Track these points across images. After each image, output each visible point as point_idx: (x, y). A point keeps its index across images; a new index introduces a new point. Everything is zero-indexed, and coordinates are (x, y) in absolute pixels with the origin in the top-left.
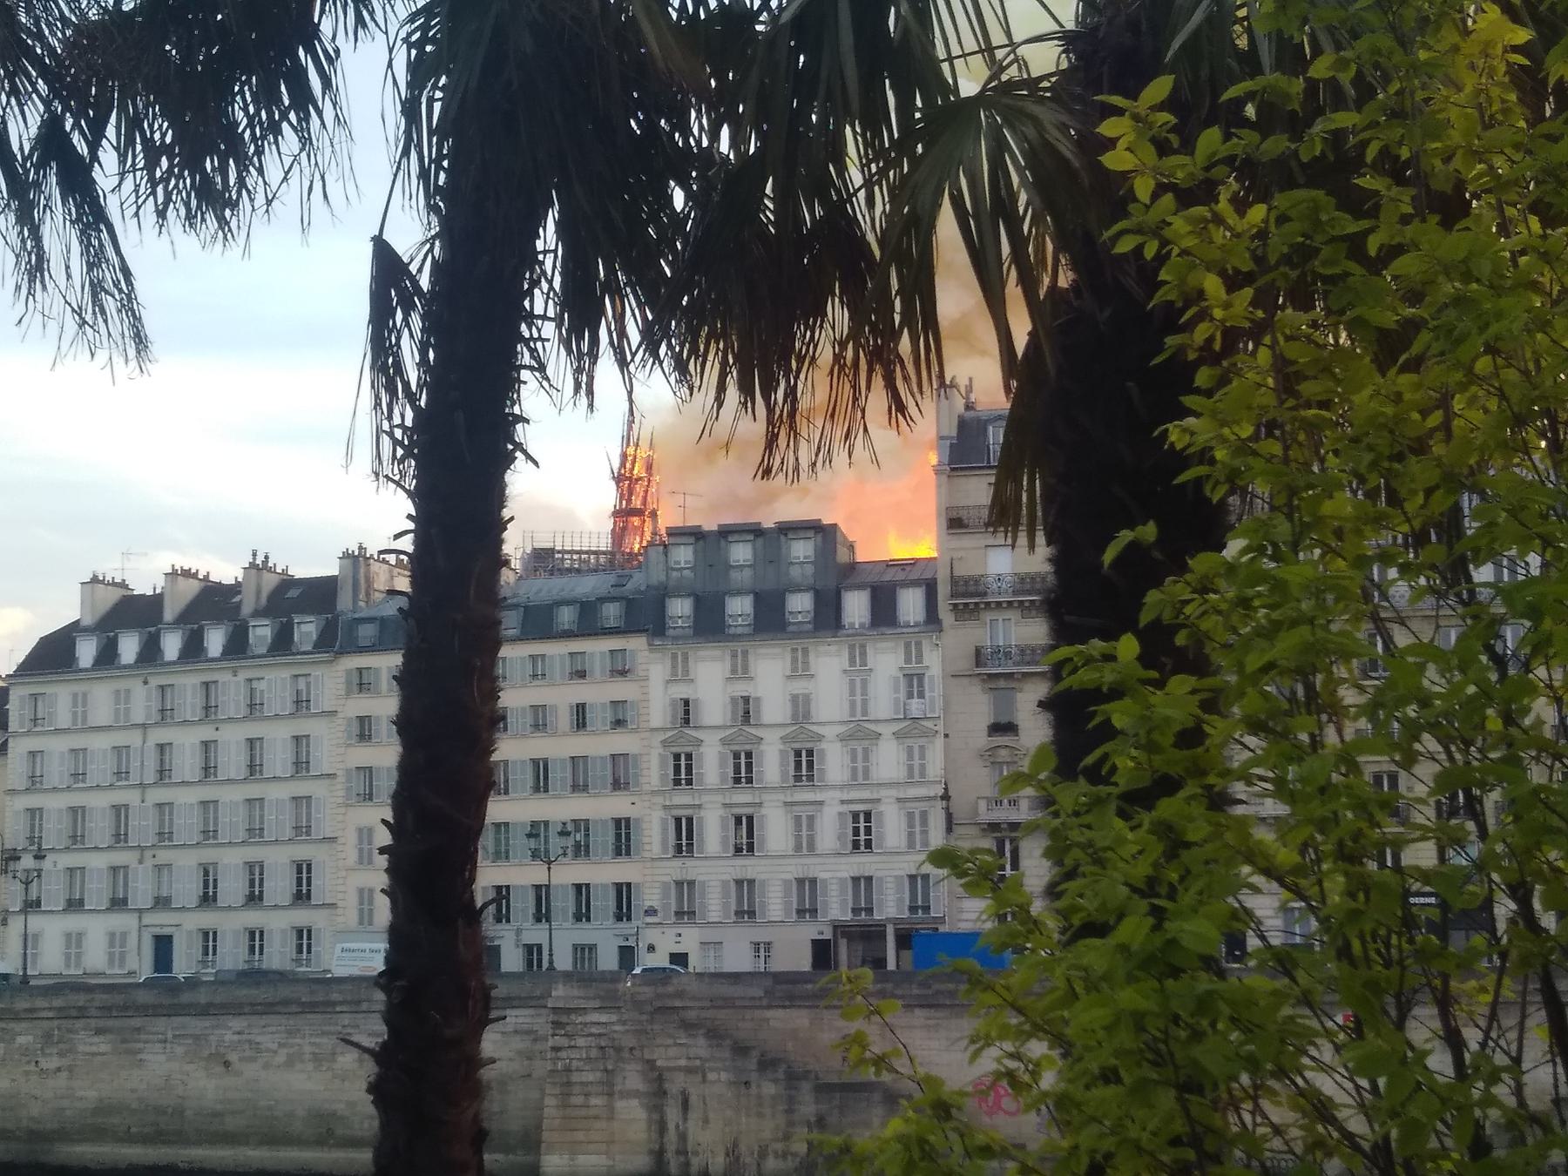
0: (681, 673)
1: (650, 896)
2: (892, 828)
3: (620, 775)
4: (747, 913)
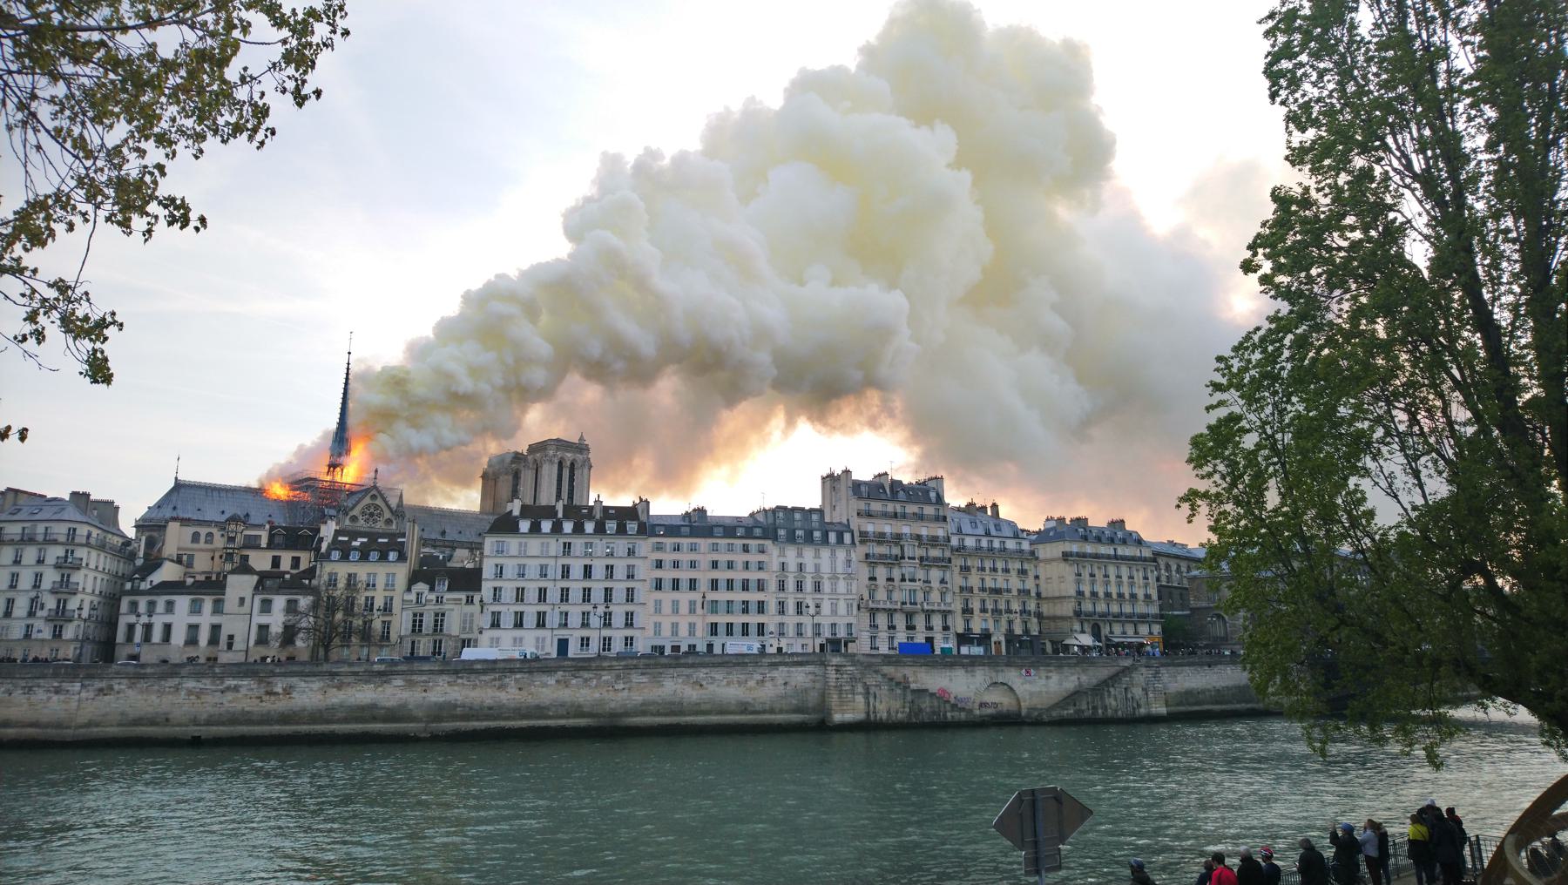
0: (782, 554)
3: (761, 586)
4: (800, 634)
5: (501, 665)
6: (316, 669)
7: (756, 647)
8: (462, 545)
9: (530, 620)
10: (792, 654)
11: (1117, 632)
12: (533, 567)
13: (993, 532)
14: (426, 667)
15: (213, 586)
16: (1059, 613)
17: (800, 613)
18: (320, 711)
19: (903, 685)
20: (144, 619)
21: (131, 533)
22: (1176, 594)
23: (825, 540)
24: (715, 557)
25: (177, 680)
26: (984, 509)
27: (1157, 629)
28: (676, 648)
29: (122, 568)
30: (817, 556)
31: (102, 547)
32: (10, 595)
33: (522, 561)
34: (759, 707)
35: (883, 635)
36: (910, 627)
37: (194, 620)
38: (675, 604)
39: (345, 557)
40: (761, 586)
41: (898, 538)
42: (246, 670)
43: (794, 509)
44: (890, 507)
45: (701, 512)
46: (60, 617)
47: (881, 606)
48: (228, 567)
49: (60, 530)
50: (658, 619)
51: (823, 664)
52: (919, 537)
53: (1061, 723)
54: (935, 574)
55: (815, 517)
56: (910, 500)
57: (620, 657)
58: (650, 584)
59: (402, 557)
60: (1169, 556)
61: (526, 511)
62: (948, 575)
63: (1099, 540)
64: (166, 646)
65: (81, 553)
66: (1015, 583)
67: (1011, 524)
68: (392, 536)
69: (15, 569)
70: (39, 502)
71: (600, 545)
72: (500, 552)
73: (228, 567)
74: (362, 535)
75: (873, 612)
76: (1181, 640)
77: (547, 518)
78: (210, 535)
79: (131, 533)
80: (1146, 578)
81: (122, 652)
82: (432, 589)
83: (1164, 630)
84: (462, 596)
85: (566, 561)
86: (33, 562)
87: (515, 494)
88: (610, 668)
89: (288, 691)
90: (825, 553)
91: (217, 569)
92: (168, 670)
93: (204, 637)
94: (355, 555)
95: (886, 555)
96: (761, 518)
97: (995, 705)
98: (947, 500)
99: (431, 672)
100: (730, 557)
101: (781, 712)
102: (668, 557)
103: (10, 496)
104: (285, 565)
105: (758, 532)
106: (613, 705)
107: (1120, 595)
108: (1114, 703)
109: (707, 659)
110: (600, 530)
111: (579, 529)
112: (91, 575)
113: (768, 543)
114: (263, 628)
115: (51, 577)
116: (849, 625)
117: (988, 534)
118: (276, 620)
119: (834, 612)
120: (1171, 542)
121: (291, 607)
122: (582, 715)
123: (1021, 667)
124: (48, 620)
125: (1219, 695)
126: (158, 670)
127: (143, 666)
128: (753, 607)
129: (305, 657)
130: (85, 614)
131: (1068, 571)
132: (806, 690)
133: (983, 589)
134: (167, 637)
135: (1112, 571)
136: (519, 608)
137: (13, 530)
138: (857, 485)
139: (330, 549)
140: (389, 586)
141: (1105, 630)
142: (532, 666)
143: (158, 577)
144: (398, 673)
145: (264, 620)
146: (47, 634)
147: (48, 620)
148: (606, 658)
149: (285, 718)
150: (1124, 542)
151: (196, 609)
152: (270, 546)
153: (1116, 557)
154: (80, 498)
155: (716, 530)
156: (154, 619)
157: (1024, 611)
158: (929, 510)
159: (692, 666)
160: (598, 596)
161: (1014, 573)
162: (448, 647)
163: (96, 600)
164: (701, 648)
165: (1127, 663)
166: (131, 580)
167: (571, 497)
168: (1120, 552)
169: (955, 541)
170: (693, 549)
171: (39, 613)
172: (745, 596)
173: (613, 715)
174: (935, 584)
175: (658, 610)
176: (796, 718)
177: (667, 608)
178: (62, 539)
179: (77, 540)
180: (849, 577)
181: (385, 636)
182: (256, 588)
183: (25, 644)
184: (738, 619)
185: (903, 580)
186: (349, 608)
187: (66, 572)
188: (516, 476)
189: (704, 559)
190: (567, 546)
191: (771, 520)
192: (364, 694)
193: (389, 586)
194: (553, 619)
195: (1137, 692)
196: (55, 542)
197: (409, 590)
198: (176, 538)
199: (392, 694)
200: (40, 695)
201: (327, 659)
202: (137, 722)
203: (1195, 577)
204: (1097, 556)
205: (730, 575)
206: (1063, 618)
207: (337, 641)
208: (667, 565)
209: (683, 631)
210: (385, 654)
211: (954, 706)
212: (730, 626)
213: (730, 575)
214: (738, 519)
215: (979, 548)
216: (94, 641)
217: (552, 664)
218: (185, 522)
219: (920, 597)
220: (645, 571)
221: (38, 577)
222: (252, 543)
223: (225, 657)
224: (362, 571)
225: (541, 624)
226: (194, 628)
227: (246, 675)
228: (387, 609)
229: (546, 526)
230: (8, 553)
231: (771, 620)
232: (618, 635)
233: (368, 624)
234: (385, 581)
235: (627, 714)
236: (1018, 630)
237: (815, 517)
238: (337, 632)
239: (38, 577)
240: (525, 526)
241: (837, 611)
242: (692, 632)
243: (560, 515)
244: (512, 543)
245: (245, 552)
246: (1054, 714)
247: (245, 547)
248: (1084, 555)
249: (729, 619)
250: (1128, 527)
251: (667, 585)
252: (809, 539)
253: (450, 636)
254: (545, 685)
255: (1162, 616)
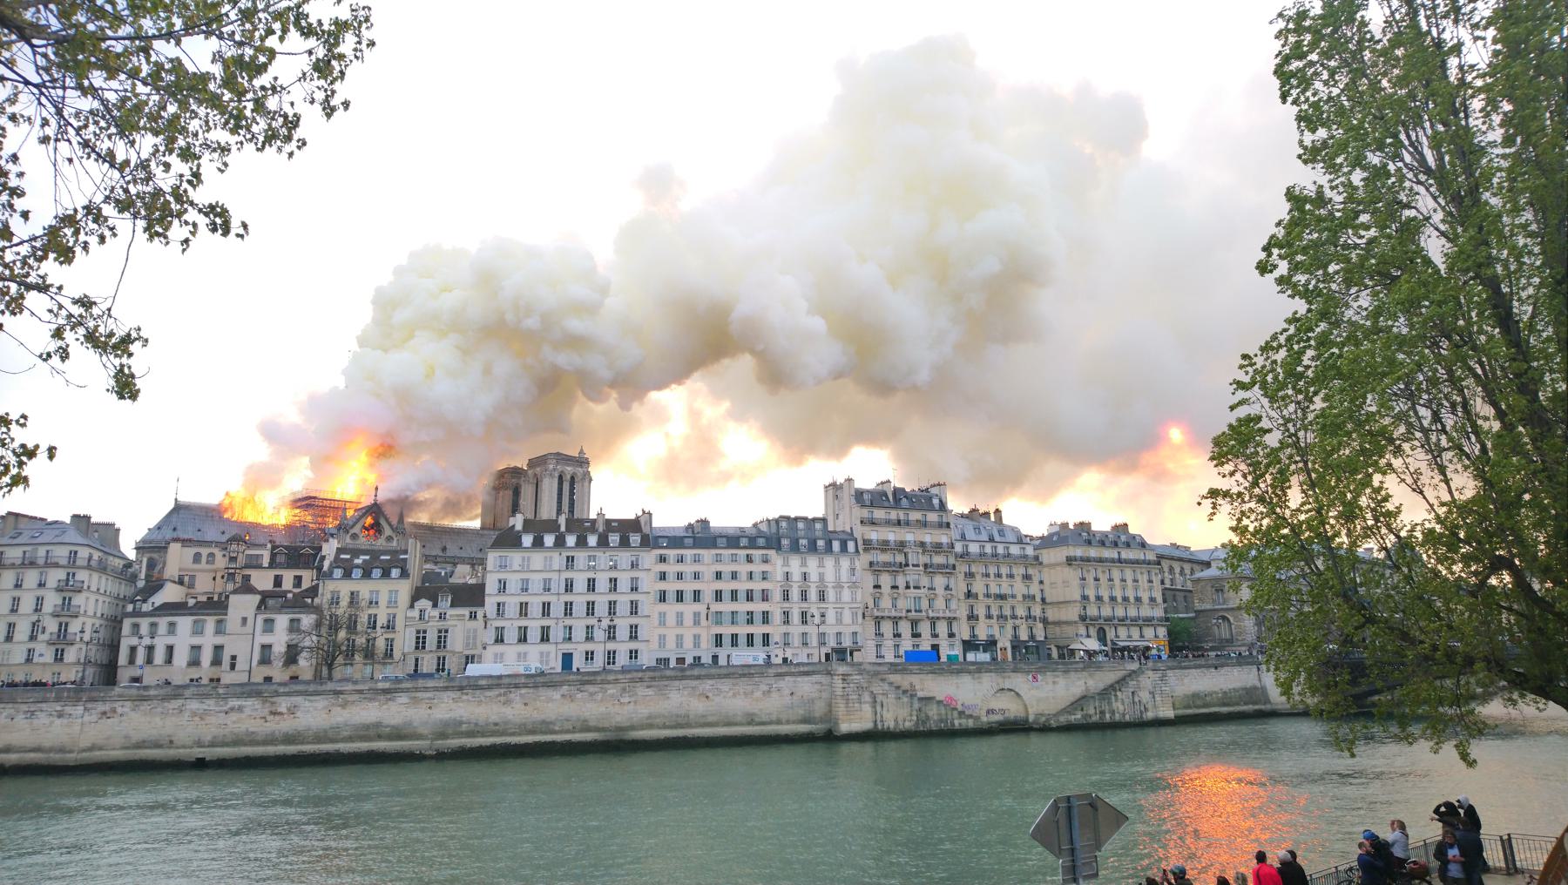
0: (786, 564)
1: (776, 638)
2: (847, 617)
3: (765, 597)
4: (805, 644)
5: (506, 681)
6: (320, 688)
7: (761, 657)
8: (463, 561)
9: (534, 635)
10: (798, 664)
11: (1125, 636)
12: (536, 581)
13: (997, 538)
14: (430, 683)
15: (216, 606)
16: (1064, 618)
17: (804, 622)
18: (325, 731)
19: (910, 693)
20: (147, 641)
21: (131, 554)
22: (1180, 596)
23: (829, 549)
24: (719, 568)
25: (180, 702)
26: (987, 514)
27: (1162, 632)
28: (681, 661)
29: (125, 590)
30: (821, 565)
31: (102, 568)
32: (12, 619)
33: (525, 576)
34: (765, 719)
35: (889, 643)
36: (916, 635)
37: (196, 641)
38: (680, 616)
39: (347, 575)
40: (765, 597)
41: (901, 546)
42: (248, 690)
43: (796, 519)
44: (893, 515)
45: (704, 523)
46: (62, 639)
47: (886, 614)
48: (230, 587)
49: (61, 553)
50: (662, 631)
51: (829, 673)
52: (922, 544)
53: (1069, 728)
54: (940, 581)
55: (818, 526)
56: (913, 507)
57: (624, 670)
58: (654, 597)
59: (404, 574)
60: (1172, 559)
61: (528, 525)
62: (952, 581)
63: (1102, 544)
64: (168, 668)
65: (82, 575)
66: (1020, 588)
67: (1014, 530)
68: (394, 553)
69: (17, 593)
70: (40, 525)
71: (603, 558)
72: (503, 567)
73: (230, 587)
74: (365, 552)
75: (878, 620)
76: (1187, 643)
77: (550, 532)
78: (212, 555)
79: (131, 554)
80: (1150, 581)
81: (124, 675)
82: (435, 605)
83: (1170, 633)
84: (465, 611)
85: (569, 575)
86: (34, 585)
87: (515, 509)
88: (616, 681)
89: (292, 711)
90: (829, 562)
91: (219, 590)
92: (172, 692)
93: (206, 657)
94: (357, 573)
95: (890, 562)
96: (764, 528)
97: (1003, 711)
98: (950, 506)
99: (436, 689)
100: (734, 567)
101: (788, 722)
102: (671, 568)
103: (12, 519)
104: (287, 584)
105: (761, 542)
106: (618, 719)
107: (1125, 599)
108: (1121, 707)
109: (713, 671)
110: (603, 542)
111: (582, 543)
112: (93, 598)
113: (772, 553)
114: (266, 648)
115: (52, 600)
116: (855, 634)
117: (991, 540)
118: (279, 639)
119: (839, 621)
120: (1174, 545)
121: (294, 626)
122: (588, 729)
123: (1028, 672)
124: (50, 643)
125: (1226, 699)
126: (162, 692)
127: (146, 688)
128: (758, 618)
129: (307, 675)
130: (87, 637)
131: (1072, 575)
132: (812, 701)
133: (988, 596)
134: (169, 660)
135: (1116, 574)
136: (523, 623)
137: (13, 554)
138: (859, 494)
139: (332, 567)
140: (392, 603)
141: (1110, 634)
142: (539, 681)
143: (159, 599)
144: (403, 691)
145: (267, 639)
146: (49, 657)
147: (50, 643)
148: (611, 671)
149: (289, 739)
150: (1128, 545)
151: (198, 630)
152: (273, 565)
153: (1120, 561)
154: (81, 521)
155: (719, 541)
156: (156, 641)
157: (1029, 617)
158: (932, 517)
159: (698, 678)
160: (601, 609)
161: (1018, 579)
162: (452, 664)
163: (98, 622)
164: (706, 659)
165: (1134, 666)
166: (133, 602)
167: (571, 511)
168: (1124, 555)
169: (958, 548)
170: (697, 560)
171: (41, 637)
172: (750, 607)
173: (620, 729)
174: (940, 591)
175: (662, 623)
176: (803, 728)
177: (671, 620)
178: (64, 562)
179: (79, 563)
180: (854, 585)
181: (389, 654)
182: (259, 608)
183: (27, 668)
184: (743, 630)
185: (908, 587)
186: (352, 626)
187: (67, 595)
188: (517, 492)
189: (708, 570)
190: (570, 560)
191: (774, 530)
192: (368, 713)
193: (392, 603)
194: (557, 633)
195: (1144, 696)
196: (56, 565)
197: (412, 606)
198: (177, 559)
199: (396, 712)
200: (42, 719)
201: (330, 678)
202: (140, 745)
203: (1199, 580)
204: (1101, 560)
205: (734, 585)
206: (1067, 623)
207: (340, 660)
208: (671, 576)
209: (688, 643)
210: (389, 671)
211: (961, 713)
212: (734, 638)
213: (734, 585)
214: (742, 529)
215: (983, 555)
216: (96, 664)
217: (557, 679)
218: (186, 542)
219: (924, 604)
220: (649, 583)
221: (39, 601)
222: (254, 564)
223: (228, 678)
224: (365, 589)
225: (545, 638)
226: (196, 649)
227: (250, 695)
228: (390, 626)
229: (549, 540)
230: (9, 577)
231: (776, 630)
232: (622, 648)
233: (371, 642)
234: (388, 597)
235: (633, 728)
236: (1024, 636)
237: (818, 526)
238: (340, 650)
239: (39, 601)
240: (527, 540)
241: (842, 620)
242: (697, 644)
243: (563, 529)
244: (515, 557)
245: (247, 572)
246: (1063, 719)
247: (247, 567)
248: (1088, 560)
249: (735, 630)
250: (1132, 530)
251: (671, 597)
252: (813, 548)
253: (453, 653)
254: (550, 700)
255: (1167, 619)
